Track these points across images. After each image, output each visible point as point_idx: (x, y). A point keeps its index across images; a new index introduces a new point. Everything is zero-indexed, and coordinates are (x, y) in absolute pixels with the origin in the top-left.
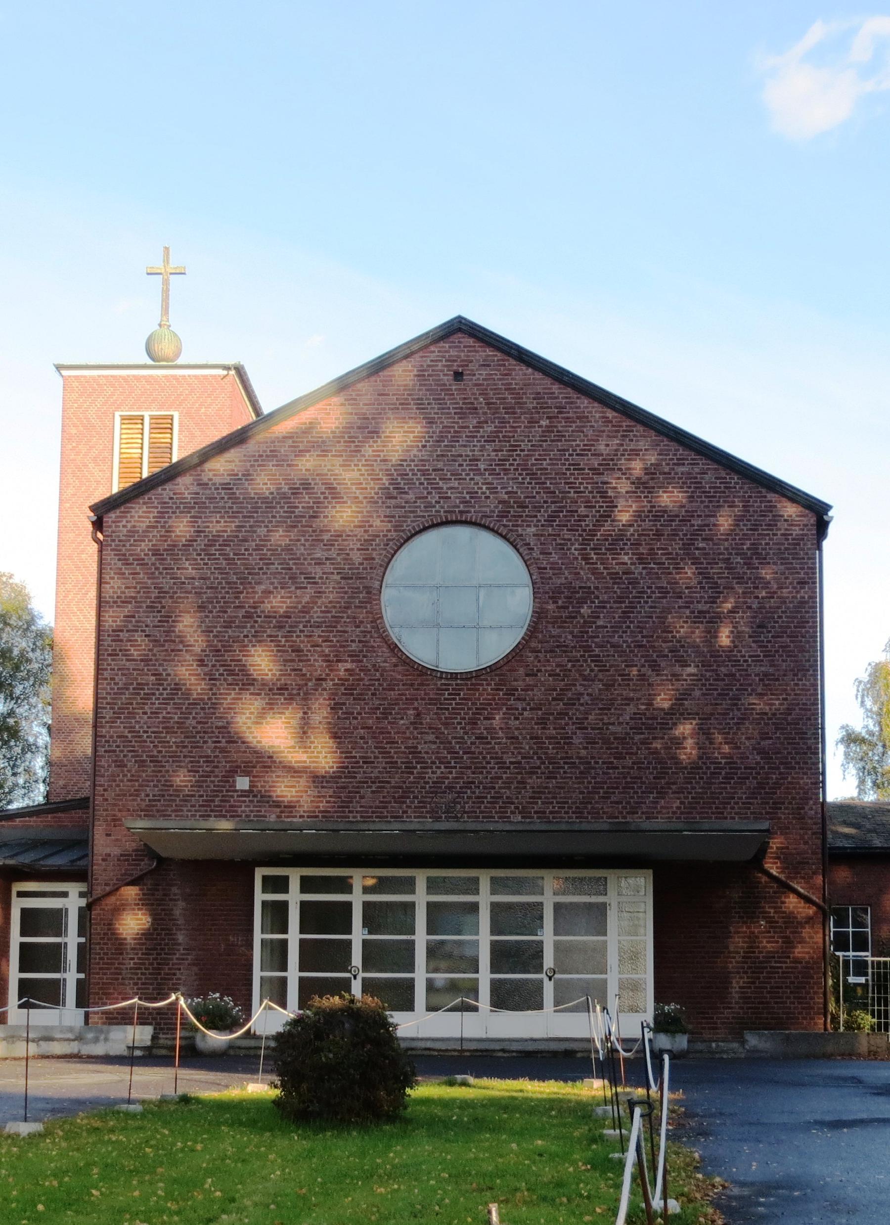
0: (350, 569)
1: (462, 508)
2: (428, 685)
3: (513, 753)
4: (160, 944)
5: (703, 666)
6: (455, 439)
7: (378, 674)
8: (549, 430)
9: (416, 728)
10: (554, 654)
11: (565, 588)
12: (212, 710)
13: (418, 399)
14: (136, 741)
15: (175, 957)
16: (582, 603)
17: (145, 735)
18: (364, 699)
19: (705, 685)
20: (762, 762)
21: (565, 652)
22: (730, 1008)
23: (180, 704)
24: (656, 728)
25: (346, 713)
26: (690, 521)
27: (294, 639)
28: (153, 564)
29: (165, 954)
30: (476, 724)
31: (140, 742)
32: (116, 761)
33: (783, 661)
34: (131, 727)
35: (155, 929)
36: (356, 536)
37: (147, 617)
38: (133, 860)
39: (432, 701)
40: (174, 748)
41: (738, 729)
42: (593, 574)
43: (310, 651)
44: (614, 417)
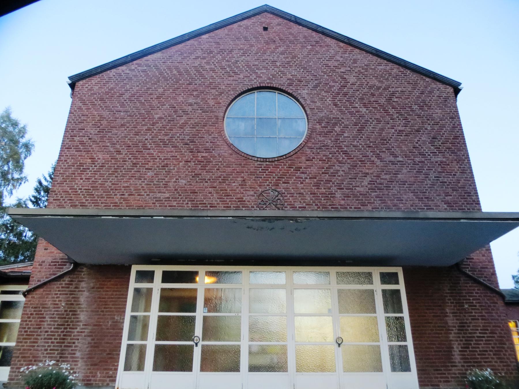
0: (206, 108)
1: (268, 81)
2: (250, 165)
3: (300, 202)
4: (67, 322)
5: (405, 157)
6: (265, 53)
7: (221, 159)
8: (311, 50)
10: (321, 150)
11: (325, 118)
12: (122, 178)
13: (245, 37)
14: (73, 194)
15: (76, 330)
16: (335, 125)
17: (80, 191)
18: (212, 172)
19: (408, 167)
20: (448, 208)
21: (327, 149)
23: (103, 174)
24: (383, 189)
25: (201, 179)
26: (388, 89)
27: (174, 141)
28: (99, 105)
29: (70, 328)
30: (278, 185)
32: (59, 205)
33: (450, 155)
35: (66, 311)
36: (211, 93)
37: (92, 130)
38: (59, 265)
39: (252, 173)
40: (96, 198)
41: (431, 190)
42: (340, 112)
43: (182, 147)
44: (344, 46)
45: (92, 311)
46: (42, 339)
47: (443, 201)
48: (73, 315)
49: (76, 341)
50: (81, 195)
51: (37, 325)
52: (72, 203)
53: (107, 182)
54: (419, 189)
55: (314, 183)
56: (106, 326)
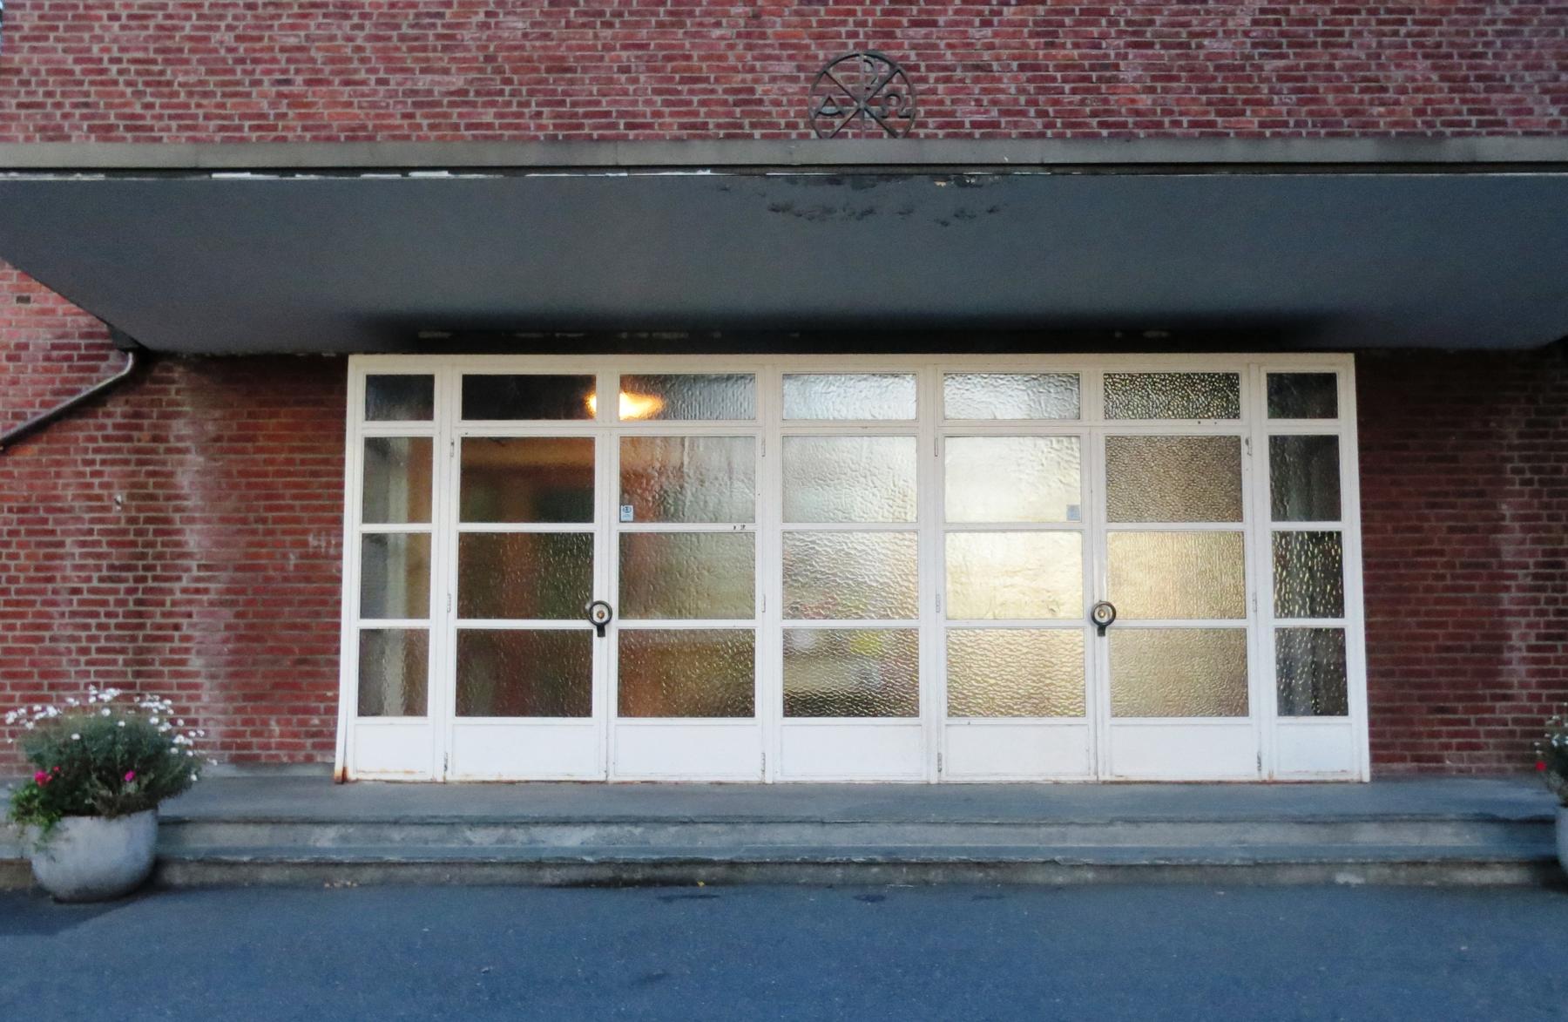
3: (979, 102)
4: (143, 556)
9: (749, 47)
12: (271, 10)
14: (92, 83)
15: (177, 586)
17: (114, 68)
22: (1506, 698)
24: (1313, 45)
25: (585, 14)
29: (155, 579)
30: (891, 35)
31: (102, 83)
32: (42, 129)
34: (81, 51)
38: (81, 358)
40: (183, 97)
41: (1506, 45)
45: (223, 520)
46: (62, 615)
47: (1545, 91)
48: (157, 533)
49: (184, 621)
50: (121, 87)
51: (38, 569)
52: (93, 117)
53: (217, 28)
54: (1458, 40)
55: (1036, 23)
56: (282, 568)
